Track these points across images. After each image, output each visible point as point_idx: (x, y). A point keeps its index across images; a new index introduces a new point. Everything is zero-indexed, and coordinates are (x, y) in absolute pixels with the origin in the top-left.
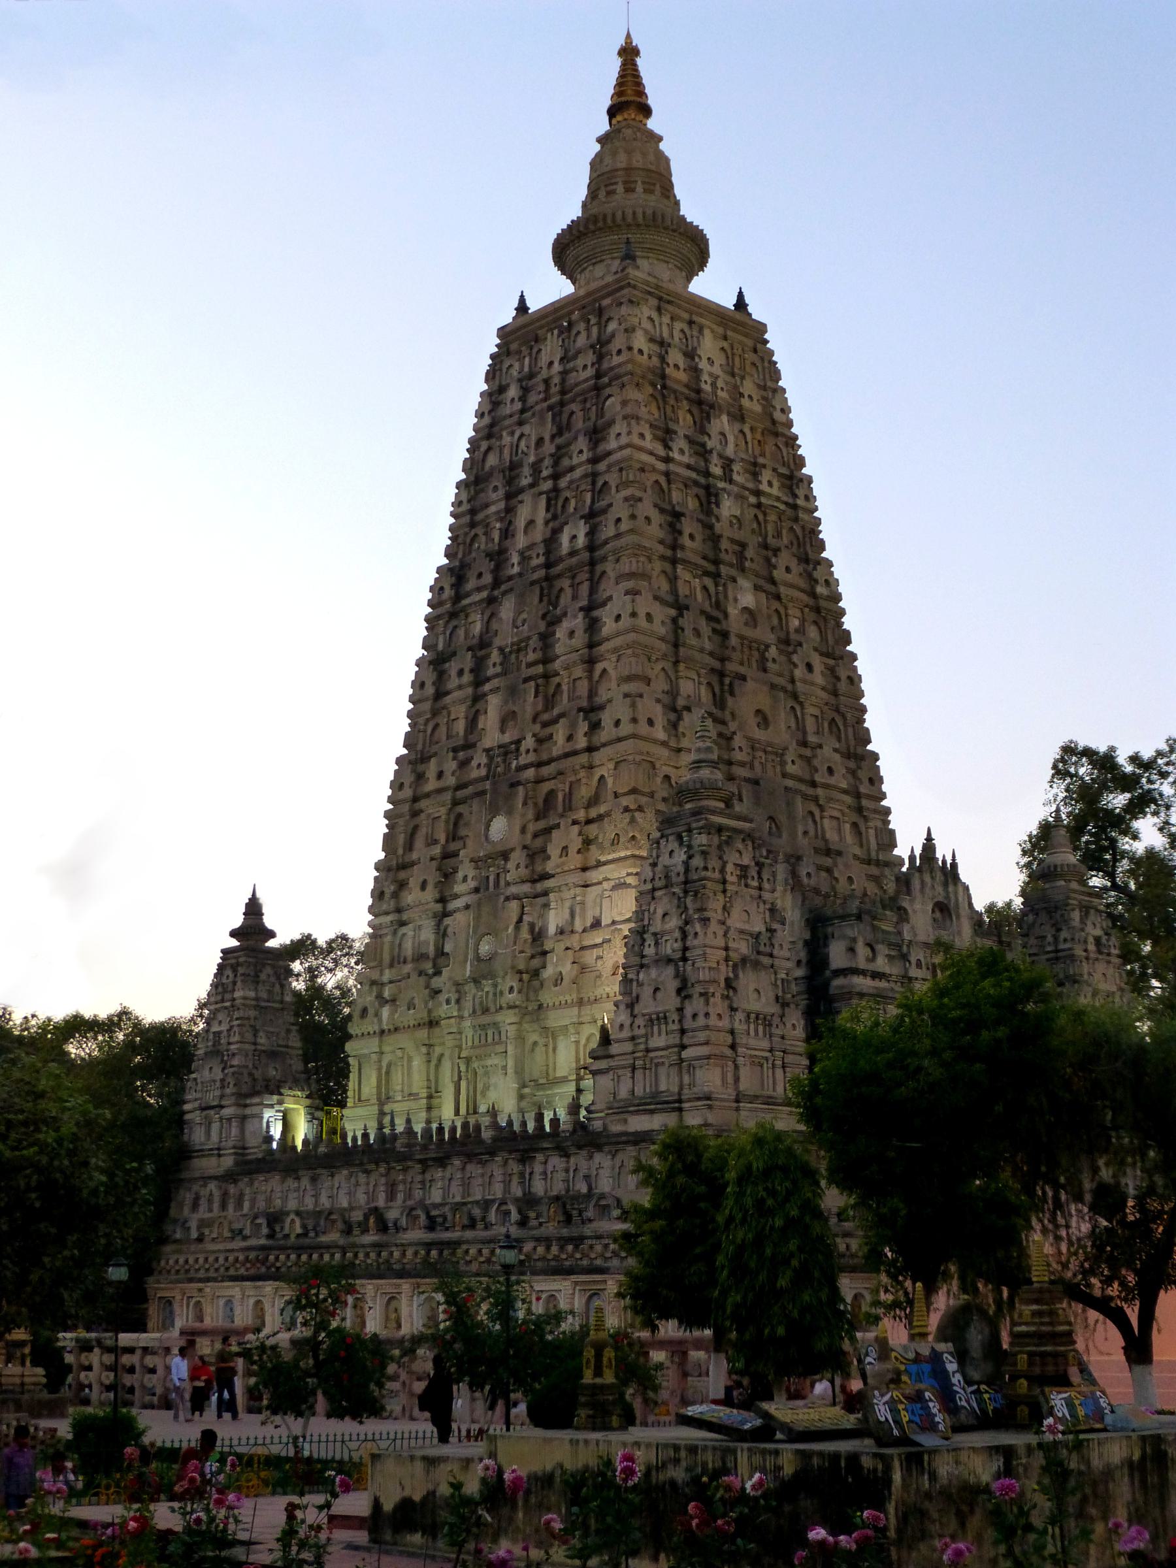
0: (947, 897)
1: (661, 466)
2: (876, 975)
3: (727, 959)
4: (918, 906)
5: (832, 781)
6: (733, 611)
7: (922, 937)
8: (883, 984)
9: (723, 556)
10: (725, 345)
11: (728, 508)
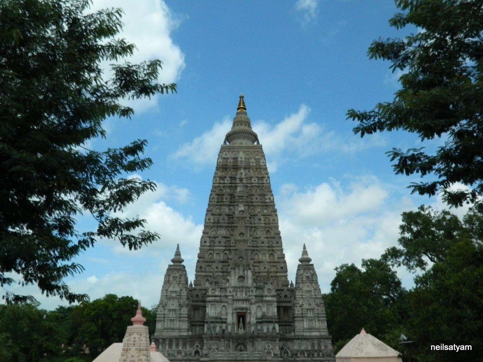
0: (244, 274)
1: (221, 185)
2: (215, 296)
3: (166, 298)
4: (232, 278)
5: (263, 245)
6: (236, 212)
7: (233, 285)
8: (217, 298)
9: (236, 200)
10: (248, 153)
11: (239, 189)
